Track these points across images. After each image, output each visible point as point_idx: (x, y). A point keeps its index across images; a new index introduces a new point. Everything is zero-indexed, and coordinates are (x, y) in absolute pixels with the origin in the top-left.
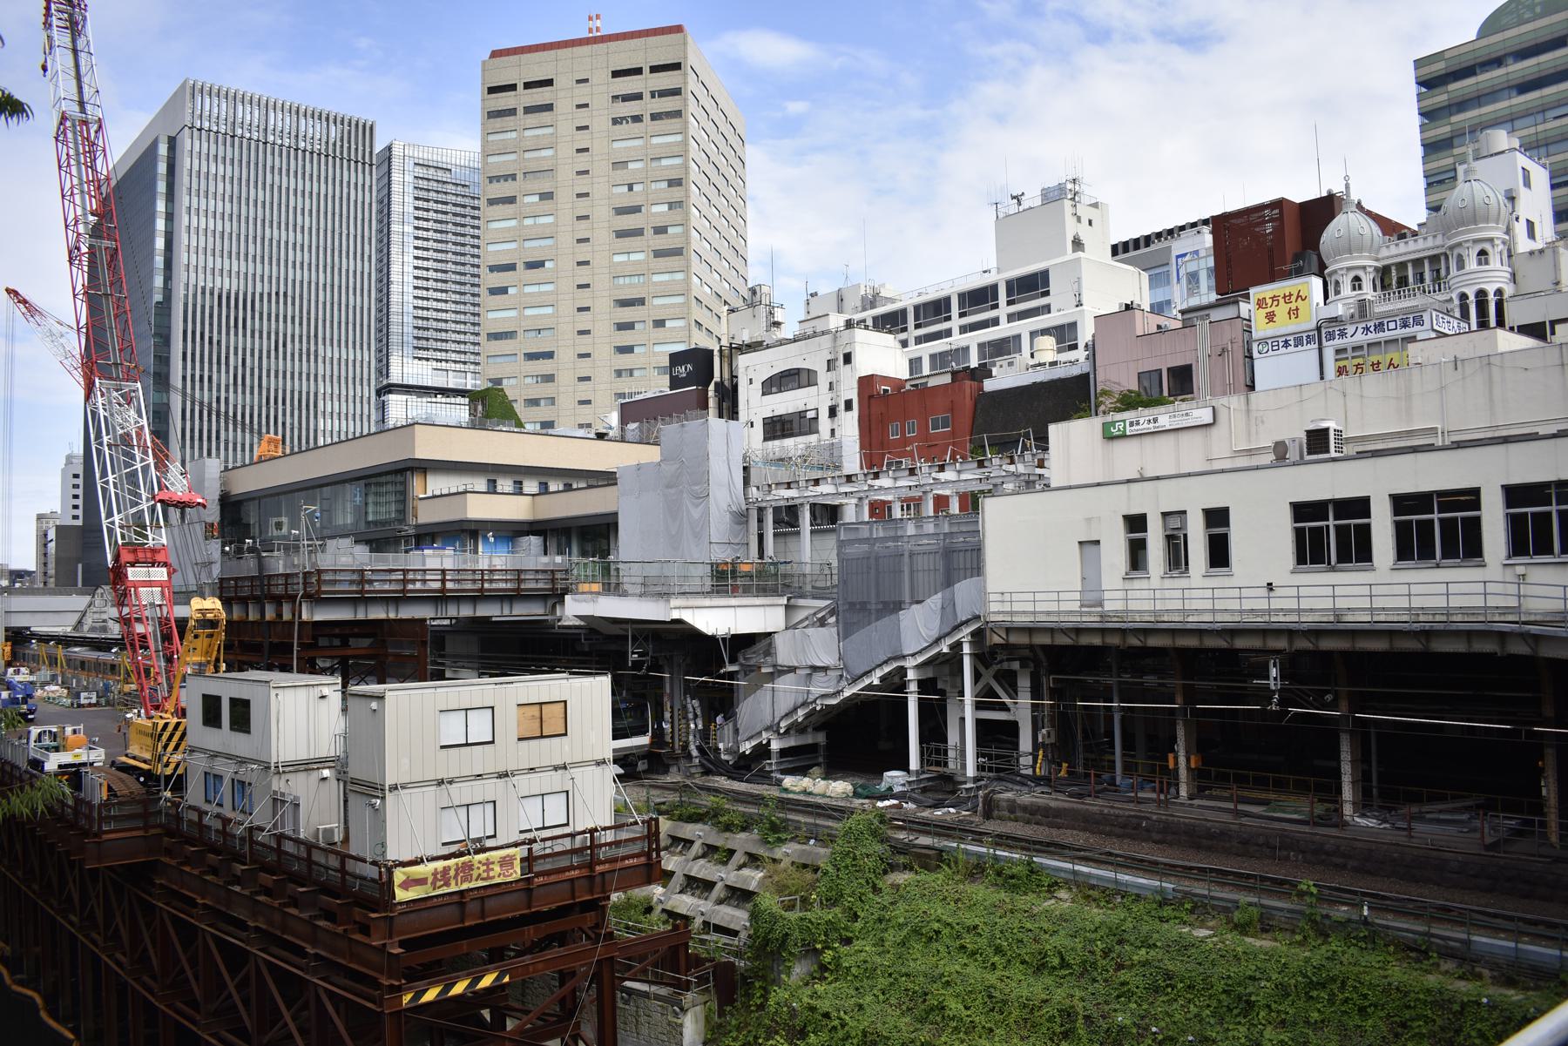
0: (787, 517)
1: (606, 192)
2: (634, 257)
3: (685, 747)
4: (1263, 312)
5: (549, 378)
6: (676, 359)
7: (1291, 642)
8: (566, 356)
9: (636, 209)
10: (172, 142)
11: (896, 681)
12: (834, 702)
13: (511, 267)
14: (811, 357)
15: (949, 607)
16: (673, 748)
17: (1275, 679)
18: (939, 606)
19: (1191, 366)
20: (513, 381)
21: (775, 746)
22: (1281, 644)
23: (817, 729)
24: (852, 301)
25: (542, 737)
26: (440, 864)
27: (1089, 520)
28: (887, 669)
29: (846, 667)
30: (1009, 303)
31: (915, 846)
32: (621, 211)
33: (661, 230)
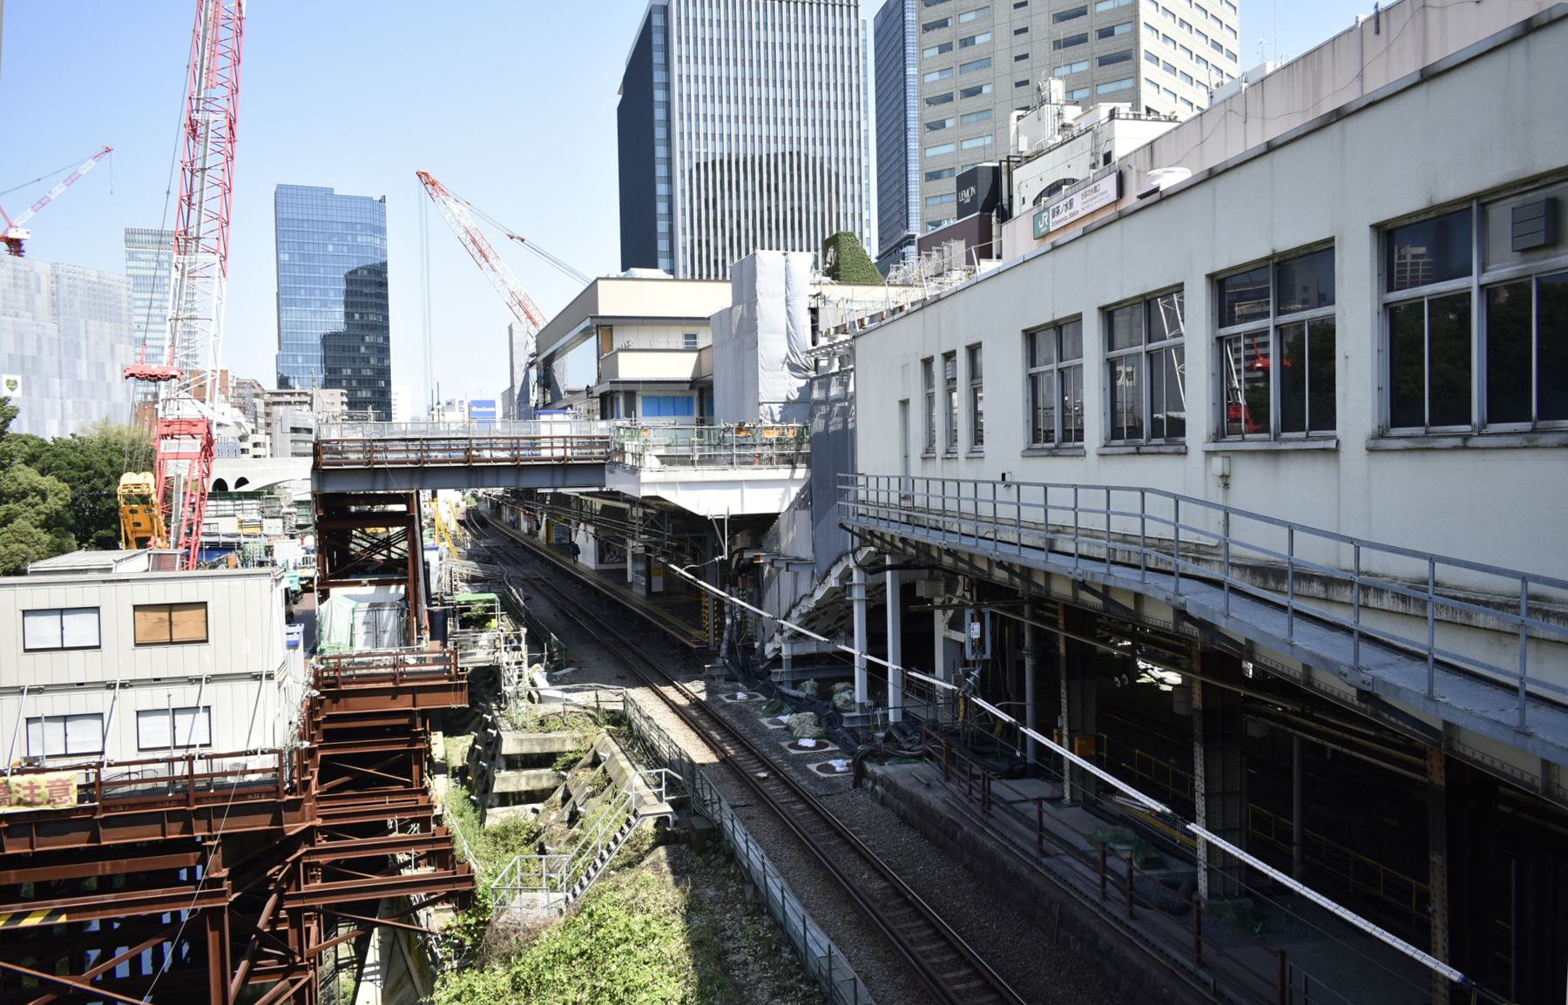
2: (1077, 68)
10: (665, 10)
13: (948, 98)
25: (171, 643)
32: (1062, 17)
33: (1106, 33)
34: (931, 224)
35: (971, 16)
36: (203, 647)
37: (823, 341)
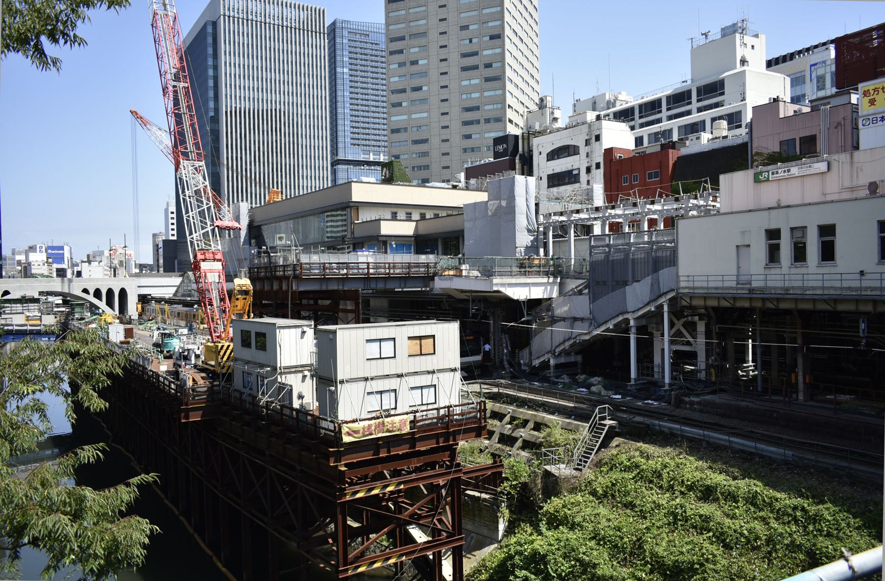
0: (562, 230)
1: (457, 44)
2: (473, 82)
3: (502, 362)
4: (867, 99)
5: (425, 154)
6: (497, 141)
7: (875, 307)
8: (435, 141)
9: (475, 54)
10: (215, 24)
11: (623, 328)
12: (587, 337)
13: (403, 91)
14: (578, 139)
15: (656, 284)
16: (495, 362)
17: (864, 330)
18: (650, 284)
19: (815, 136)
20: (406, 156)
21: (552, 362)
22: (869, 308)
23: (577, 353)
24: (602, 105)
26: (367, 423)
27: (743, 233)
28: (620, 318)
29: (594, 318)
30: (698, 101)
31: (633, 422)
32: (465, 55)
33: (488, 66)
34: (393, 156)
35: (416, 50)
36: (433, 356)
37: (541, 218)
